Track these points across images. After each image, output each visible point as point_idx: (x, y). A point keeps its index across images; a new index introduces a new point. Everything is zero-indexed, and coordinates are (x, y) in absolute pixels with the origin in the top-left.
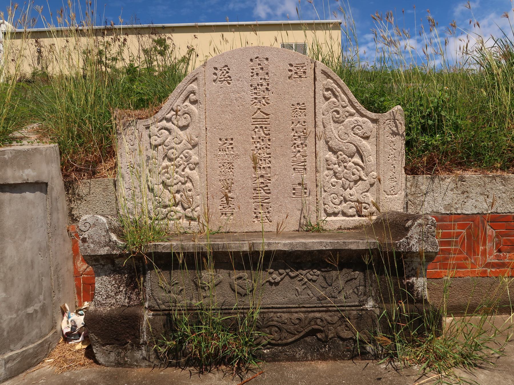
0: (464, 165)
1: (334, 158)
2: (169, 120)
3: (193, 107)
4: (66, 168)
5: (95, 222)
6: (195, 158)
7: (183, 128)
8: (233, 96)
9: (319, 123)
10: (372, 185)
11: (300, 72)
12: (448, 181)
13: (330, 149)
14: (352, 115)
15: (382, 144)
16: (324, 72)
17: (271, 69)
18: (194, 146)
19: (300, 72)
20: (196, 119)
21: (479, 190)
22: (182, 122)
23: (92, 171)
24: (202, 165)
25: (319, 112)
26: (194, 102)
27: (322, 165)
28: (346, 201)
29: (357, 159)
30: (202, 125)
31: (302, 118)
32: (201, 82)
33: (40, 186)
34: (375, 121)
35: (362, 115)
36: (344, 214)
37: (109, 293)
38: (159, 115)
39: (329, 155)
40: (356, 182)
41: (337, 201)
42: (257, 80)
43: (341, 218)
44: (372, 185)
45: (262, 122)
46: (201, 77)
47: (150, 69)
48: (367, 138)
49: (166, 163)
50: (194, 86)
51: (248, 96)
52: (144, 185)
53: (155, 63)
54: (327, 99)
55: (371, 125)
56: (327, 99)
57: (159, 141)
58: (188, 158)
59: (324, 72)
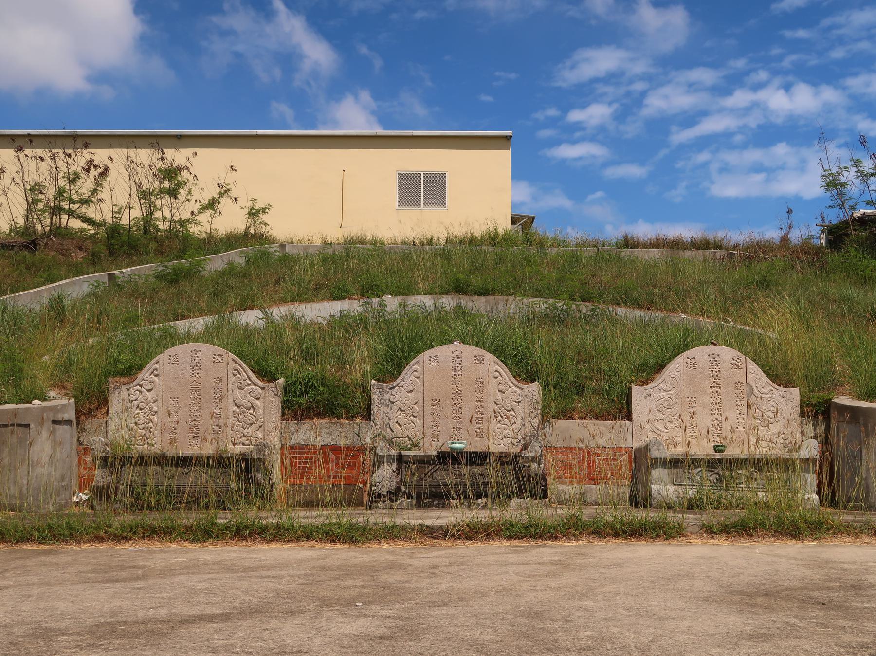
0: (320, 415)
1: (238, 410)
2: (141, 386)
3: (156, 378)
4: (78, 412)
5: (97, 441)
6: (155, 409)
7: (149, 391)
8: (180, 372)
9: (230, 390)
10: (260, 427)
11: (220, 359)
12: (307, 424)
13: (236, 405)
14: (249, 385)
15: (267, 402)
16: (233, 360)
17: (203, 357)
18: (155, 401)
19: (220, 359)
20: (157, 385)
21: (326, 430)
22: (149, 387)
23: (91, 414)
24: (159, 413)
25: (230, 382)
26: (156, 376)
27: (231, 414)
28: (244, 436)
29: (251, 411)
30: (160, 389)
31: (220, 386)
32: (161, 364)
33: (69, 422)
34: (263, 389)
35: (255, 385)
36: (243, 444)
37: (100, 477)
38: (135, 383)
39: (235, 408)
40: (251, 424)
41: (239, 436)
42: (194, 363)
43: (241, 446)
44: (260, 427)
45: (196, 388)
46: (161, 361)
47: (148, 221)
48: (258, 399)
49: (138, 411)
50: (157, 366)
51: (189, 372)
52: (124, 424)
53: (158, 214)
54: (235, 375)
55: (261, 391)
56: (235, 375)
57: (134, 398)
58: (151, 409)
59: (233, 360)
